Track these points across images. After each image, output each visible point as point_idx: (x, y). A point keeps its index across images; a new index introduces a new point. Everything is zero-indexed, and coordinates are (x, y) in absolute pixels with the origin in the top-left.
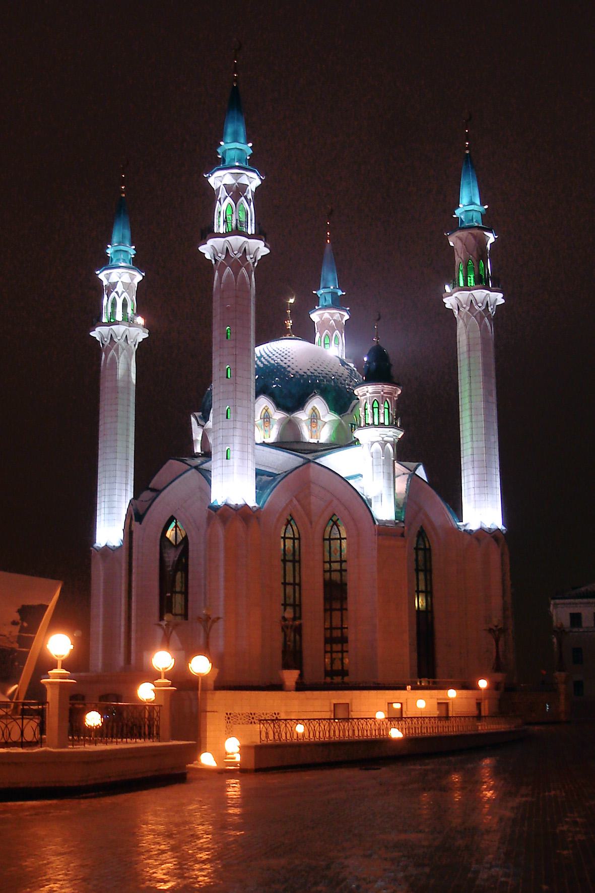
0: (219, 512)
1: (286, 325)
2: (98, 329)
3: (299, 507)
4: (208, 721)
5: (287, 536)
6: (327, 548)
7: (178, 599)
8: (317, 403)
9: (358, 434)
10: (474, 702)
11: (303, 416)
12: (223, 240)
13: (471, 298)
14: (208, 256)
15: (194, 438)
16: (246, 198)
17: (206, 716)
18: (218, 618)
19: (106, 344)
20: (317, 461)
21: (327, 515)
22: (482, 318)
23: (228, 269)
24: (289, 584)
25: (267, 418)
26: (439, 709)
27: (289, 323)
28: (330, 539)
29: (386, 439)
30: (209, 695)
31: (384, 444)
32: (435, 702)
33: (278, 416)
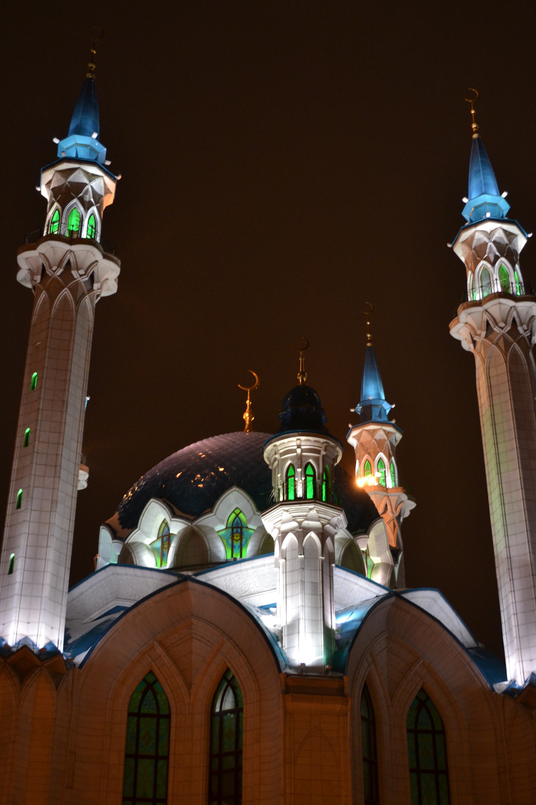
3: (166, 660)
13: (486, 317)
16: (81, 200)
20: (202, 578)
22: (507, 344)
29: (306, 523)
33: (177, 527)
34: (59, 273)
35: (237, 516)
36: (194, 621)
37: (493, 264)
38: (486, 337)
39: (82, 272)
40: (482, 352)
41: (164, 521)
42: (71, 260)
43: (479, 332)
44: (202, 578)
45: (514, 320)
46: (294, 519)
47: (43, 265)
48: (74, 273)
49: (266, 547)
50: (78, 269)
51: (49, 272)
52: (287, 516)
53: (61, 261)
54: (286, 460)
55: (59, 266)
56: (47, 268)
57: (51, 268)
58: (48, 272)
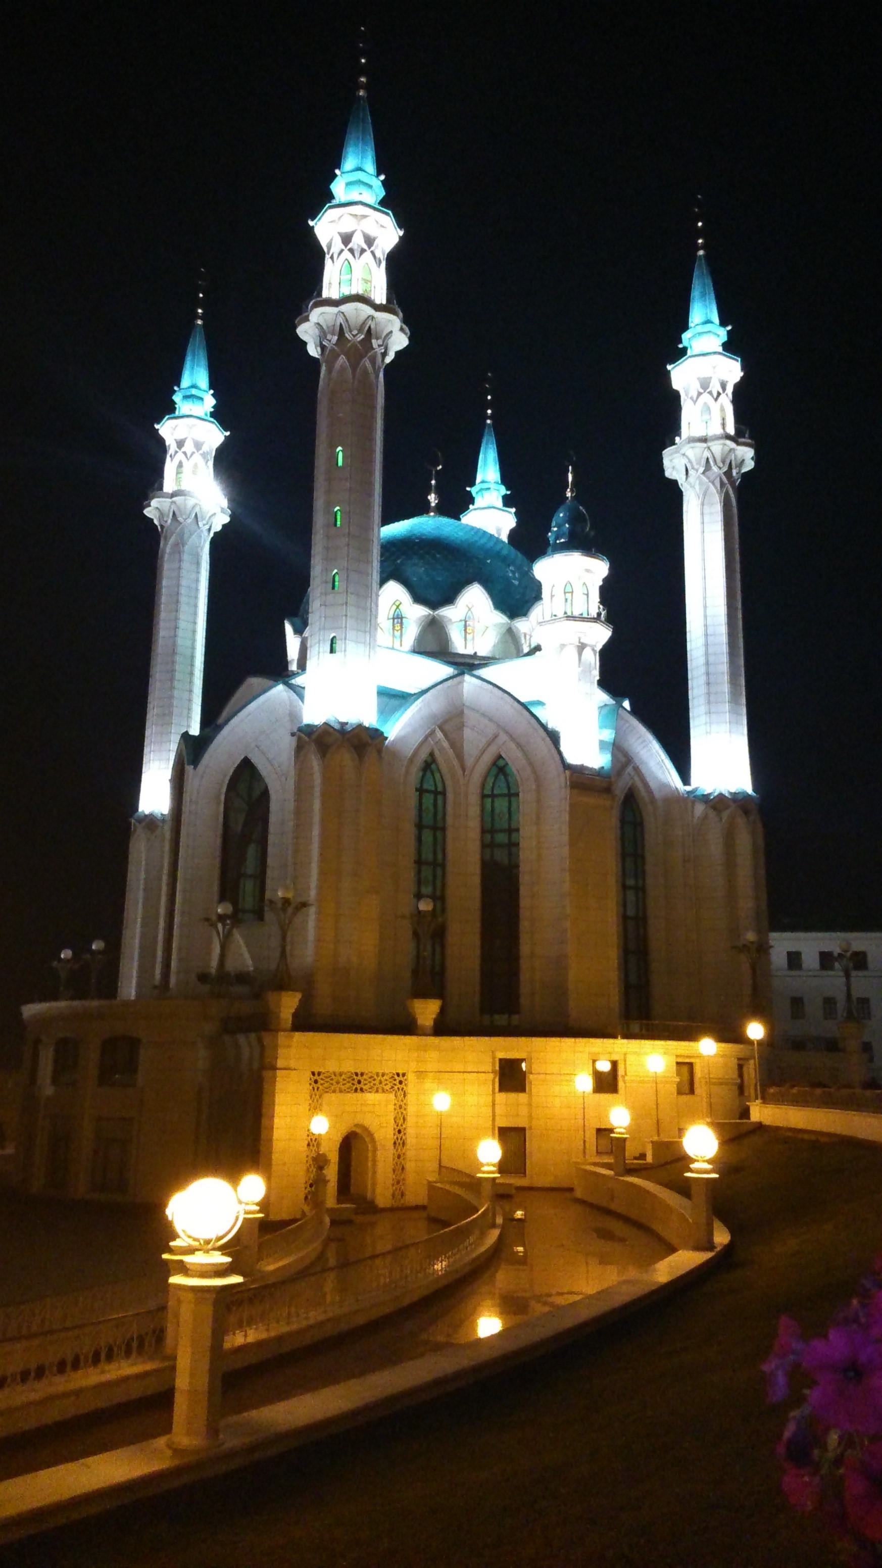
0: (314, 737)
1: (429, 502)
2: (154, 503)
3: (446, 744)
4: (279, 1085)
5: (425, 786)
8: (475, 599)
10: (734, 1063)
12: (334, 310)
13: (707, 454)
14: (313, 351)
15: (289, 658)
17: (275, 1077)
18: (304, 905)
19: (166, 525)
21: (488, 758)
22: (722, 484)
23: (342, 359)
24: (427, 863)
25: (398, 619)
26: (678, 1073)
27: (433, 498)
28: (493, 796)
30: (282, 1037)
31: (581, 647)
32: (673, 1060)
33: (416, 613)
34: (359, 339)
35: (470, 609)
38: (703, 473)
39: (380, 342)
40: (697, 487)
42: (372, 327)
43: (696, 467)
44: (476, 672)
45: (730, 464)
47: (341, 325)
48: (374, 341)
50: (377, 339)
51: (348, 336)
56: (346, 329)
57: (351, 331)
58: (347, 335)
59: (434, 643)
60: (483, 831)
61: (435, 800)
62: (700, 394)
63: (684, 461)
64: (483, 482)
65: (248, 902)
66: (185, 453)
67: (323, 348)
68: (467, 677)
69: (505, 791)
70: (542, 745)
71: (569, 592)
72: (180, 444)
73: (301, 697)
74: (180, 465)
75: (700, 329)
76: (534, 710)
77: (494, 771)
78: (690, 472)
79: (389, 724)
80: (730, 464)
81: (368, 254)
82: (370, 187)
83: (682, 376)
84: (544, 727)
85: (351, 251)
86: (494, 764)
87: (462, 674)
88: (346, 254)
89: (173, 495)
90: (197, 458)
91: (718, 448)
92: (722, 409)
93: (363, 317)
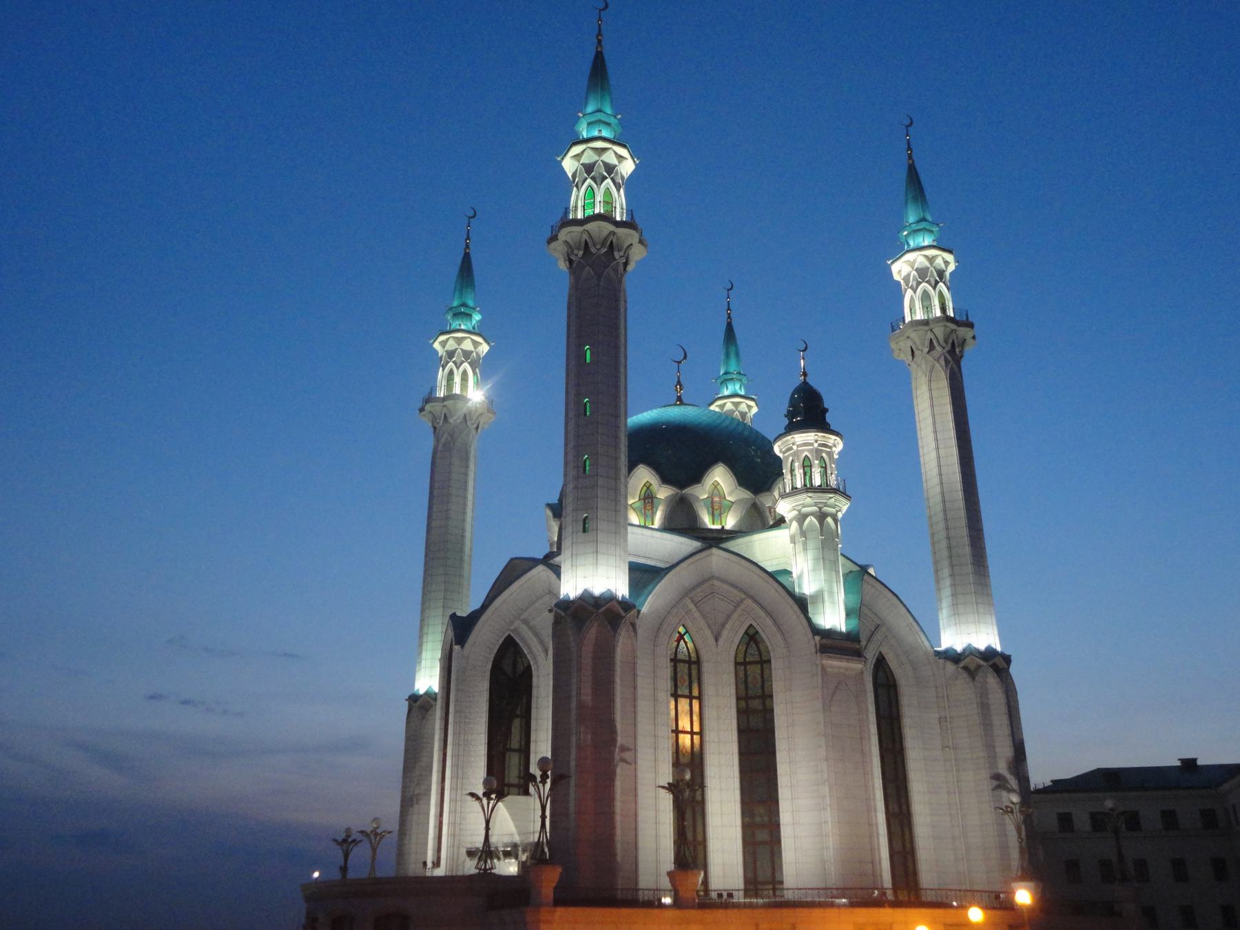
0: (569, 612)
5: (680, 656)
6: (742, 674)
7: (514, 760)
8: (720, 478)
9: (785, 508)
11: (701, 493)
13: (930, 335)
16: (613, 180)
22: (947, 361)
24: (685, 732)
29: (825, 509)
33: (663, 493)
36: (716, 583)
37: (934, 288)
41: (648, 486)
45: (953, 343)
46: (816, 504)
49: (780, 522)
51: (593, 250)
52: (809, 501)
53: (606, 239)
54: (803, 451)
55: (603, 245)
59: (682, 520)
60: (738, 699)
61: (690, 669)
62: (919, 284)
63: (909, 343)
64: (726, 373)
65: (513, 775)
66: (455, 363)
67: (571, 261)
68: (715, 551)
69: (757, 658)
70: (792, 611)
71: (807, 466)
72: (451, 354)
73: (558, 575)
74: (451, 373)
75: (914, 227)
76: (780, 579)
77: (747, 638)
78: (916, 352)
79: (642, 599)
80: (953, 343)
81: (609, 180)
82: (608, 124)
83: (901, 269)
84: (791, 594)
85: (593, 179)
86: (746, 633)
87: (710, 547)
88: (589, 180)
89: (444, 399)
90: (466, 365)
91: (939, 331)
92: (941, 295)
93: (605, 233)
